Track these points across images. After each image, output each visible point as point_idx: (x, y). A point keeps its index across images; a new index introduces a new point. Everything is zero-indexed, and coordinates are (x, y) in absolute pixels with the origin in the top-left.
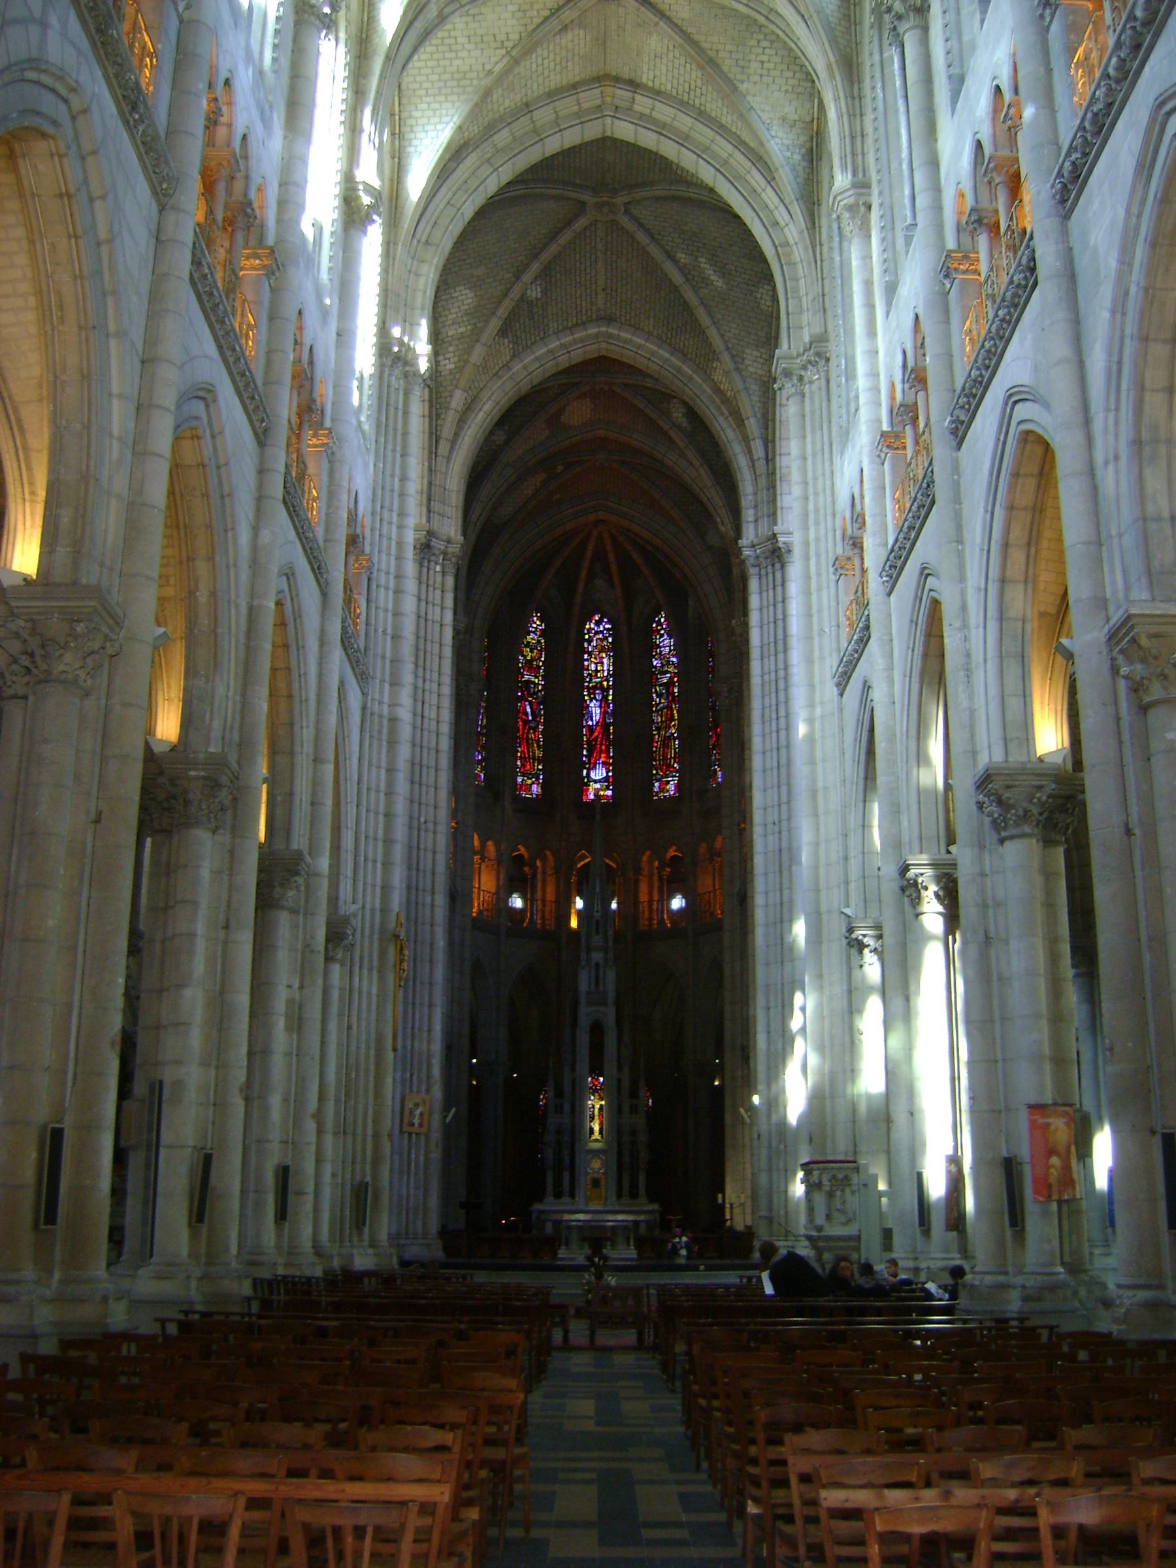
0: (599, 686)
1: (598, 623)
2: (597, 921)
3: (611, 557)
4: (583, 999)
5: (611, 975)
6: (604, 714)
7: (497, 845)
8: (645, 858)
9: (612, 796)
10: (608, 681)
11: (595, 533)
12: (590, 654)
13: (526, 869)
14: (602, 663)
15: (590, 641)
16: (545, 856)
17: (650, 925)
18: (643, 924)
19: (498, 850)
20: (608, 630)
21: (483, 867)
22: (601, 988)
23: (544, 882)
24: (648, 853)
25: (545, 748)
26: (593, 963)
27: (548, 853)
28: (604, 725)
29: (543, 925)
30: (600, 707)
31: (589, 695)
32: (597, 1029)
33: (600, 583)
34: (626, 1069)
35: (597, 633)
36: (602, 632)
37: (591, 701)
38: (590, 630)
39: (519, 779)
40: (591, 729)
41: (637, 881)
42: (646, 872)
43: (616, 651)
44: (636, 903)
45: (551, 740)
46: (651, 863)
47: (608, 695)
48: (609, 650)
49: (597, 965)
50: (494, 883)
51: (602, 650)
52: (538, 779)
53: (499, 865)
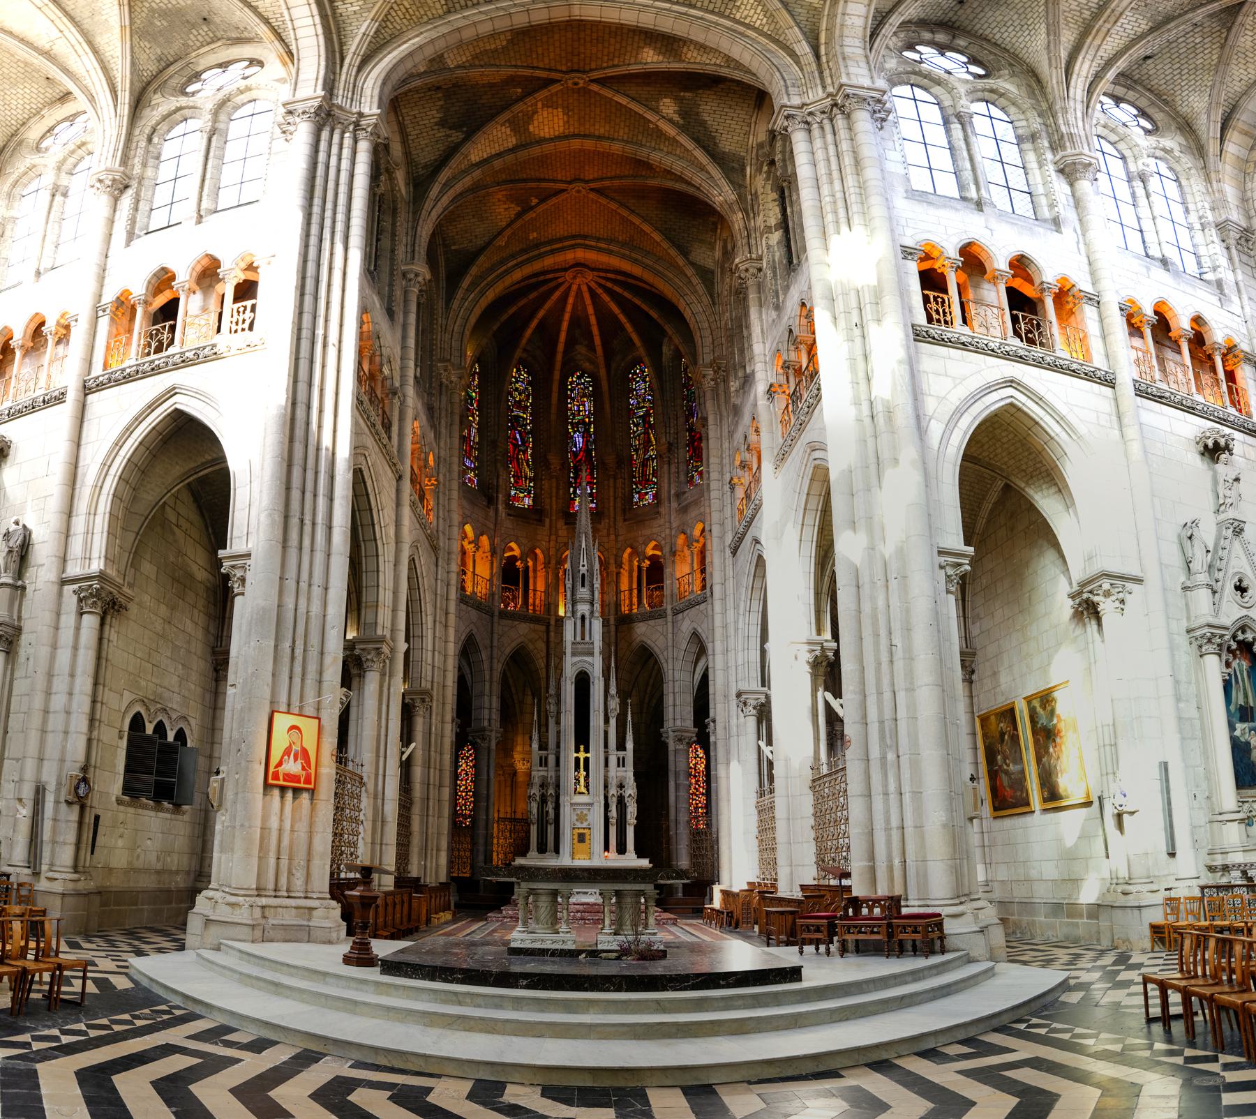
0: (583, 421)
1: (579, 378)
2: (583, 575)
3: (590, 310)
4: (568, 650)
5: (597, 626)
6: (586, 443)
7: (492, 540)
8: (626, 555)
9: (596, 508)
10: (590, 418)
11: (574, 288)
12: (573, 399)
13: (518, 563)
14: (584, 406)
15: (572, 390)
16: (536, 555)
17: (631, 610)
18: (625, 609)
19: (492, 544)
20: (588, 382)
21: (478, 554)
22: (587, 638)
23: (535, 577)
24: (629, 550)
25: (534, 467)
26: (579, 615)
27: (538, 551)
28: (587, 451)
29: (534, 610)
30: (583, 437)
31: (572, 428)
32: (583, 682)
33: (581, 349)
34: (613, 722)
35: (578, 384)
36: (583, 384)
37: (575, 432)
38: (572, 383)
39: (513, 492)
40: (575, 454)
41: (618, 574)
42: (626, 567)
43: (596, 396)
44: (618, 592)
45: (540, 461)
46: (630, 561)
47: (590, 428)
48: (590, 396)
49: (583, 618)
50: (488, 572)
51: (584, 395)
52: (529, 492)
53: (492, 556)
